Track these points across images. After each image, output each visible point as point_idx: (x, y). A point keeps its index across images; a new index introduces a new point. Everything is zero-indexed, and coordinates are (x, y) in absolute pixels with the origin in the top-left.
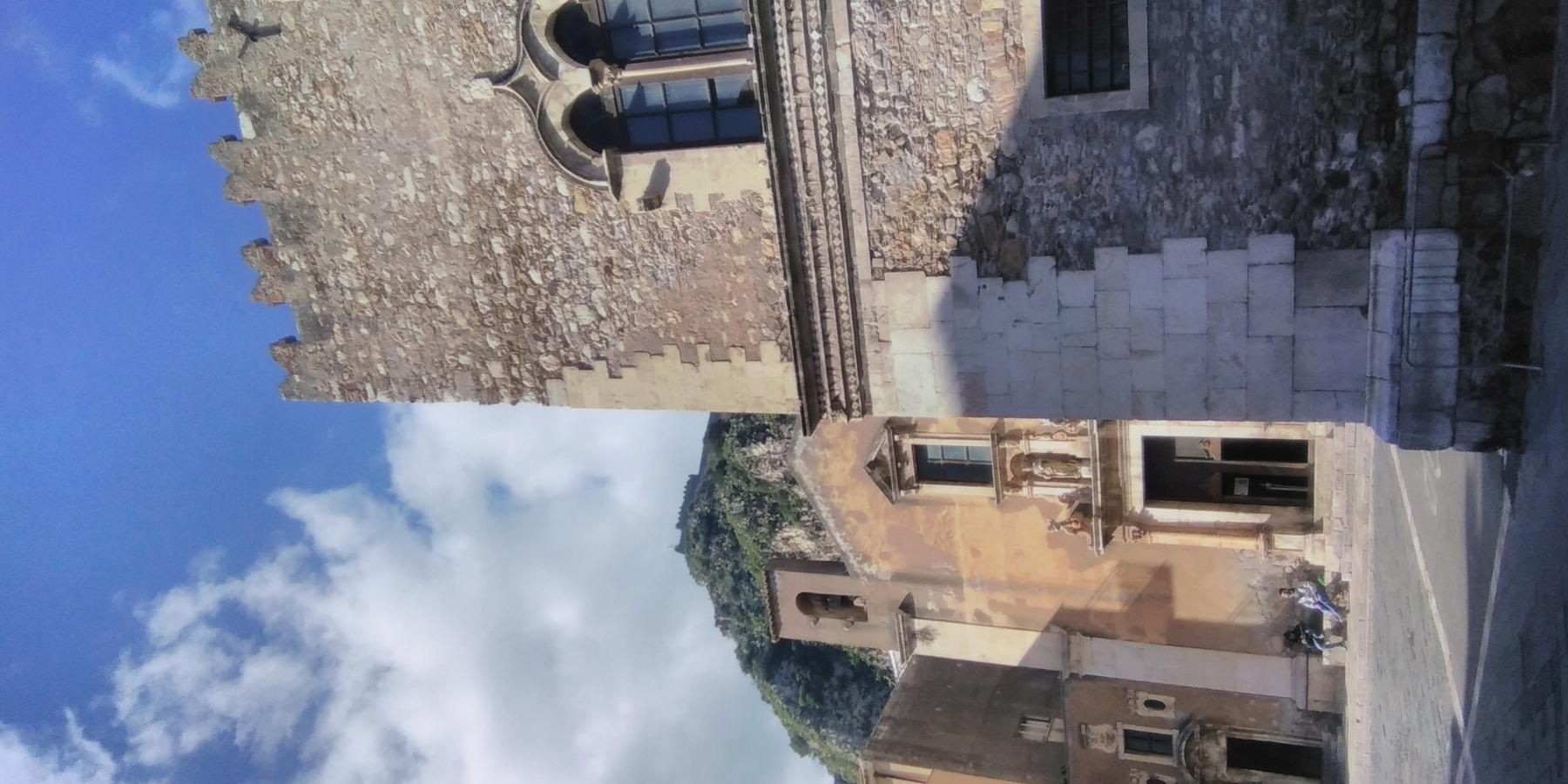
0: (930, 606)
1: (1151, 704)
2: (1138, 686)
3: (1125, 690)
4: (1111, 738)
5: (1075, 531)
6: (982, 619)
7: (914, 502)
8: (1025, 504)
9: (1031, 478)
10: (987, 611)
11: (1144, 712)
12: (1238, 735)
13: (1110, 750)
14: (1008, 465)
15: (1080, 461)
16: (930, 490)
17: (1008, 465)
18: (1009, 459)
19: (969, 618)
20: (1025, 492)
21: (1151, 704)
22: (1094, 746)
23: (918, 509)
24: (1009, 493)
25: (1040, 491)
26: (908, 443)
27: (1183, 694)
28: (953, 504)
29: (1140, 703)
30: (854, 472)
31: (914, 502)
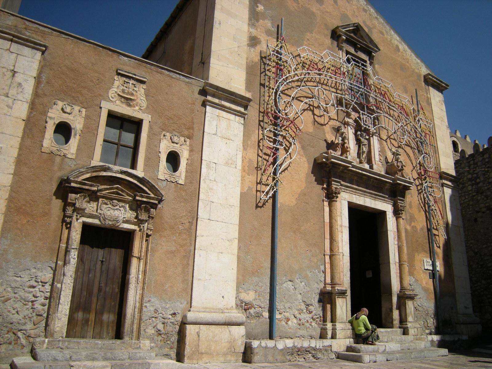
0: (260, 8)
1: (173, 159)
2: (198, 150)
3: (189, 137)
4: (128, 101)
6: (253, 41)
10: (258, 48)
11: (165, 147)
12: (138, 246)
13: (112, 93)
19: (254, 32)
21: (173, 159)
22: (118, 81)
27: (192, 192)
29: (176, 148)
30: (344, 16)
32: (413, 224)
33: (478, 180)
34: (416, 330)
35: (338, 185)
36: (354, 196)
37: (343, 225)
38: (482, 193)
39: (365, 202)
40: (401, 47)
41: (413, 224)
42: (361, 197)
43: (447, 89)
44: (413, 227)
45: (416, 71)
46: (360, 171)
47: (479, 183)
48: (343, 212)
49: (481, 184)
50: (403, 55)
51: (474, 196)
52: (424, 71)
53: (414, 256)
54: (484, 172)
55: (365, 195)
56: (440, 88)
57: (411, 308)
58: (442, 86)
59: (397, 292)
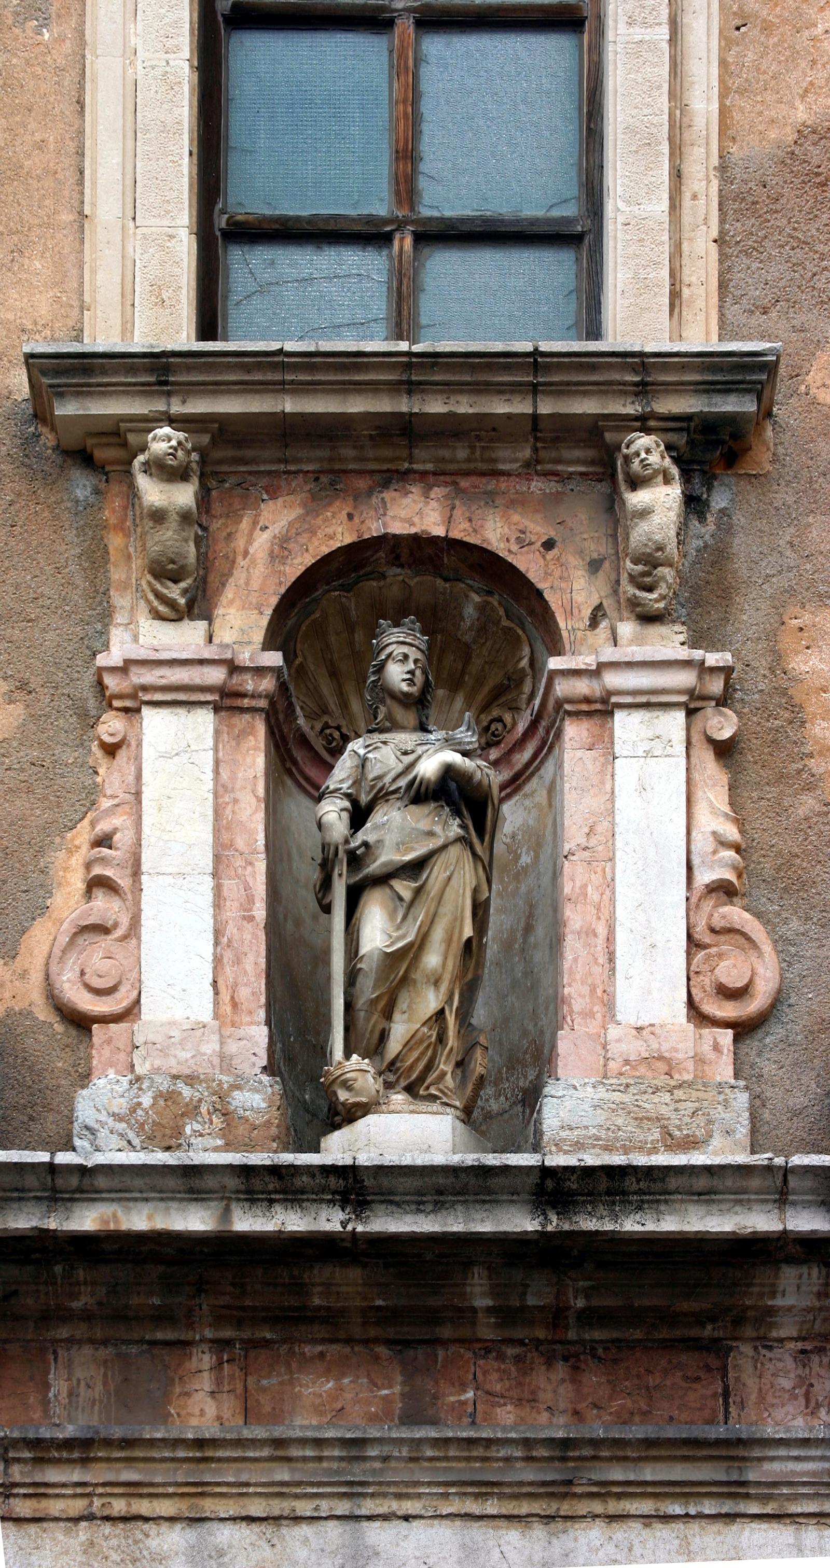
9: (299, 719)
14: (416, 513)
25: (186, 786)
42: (305, 1530)
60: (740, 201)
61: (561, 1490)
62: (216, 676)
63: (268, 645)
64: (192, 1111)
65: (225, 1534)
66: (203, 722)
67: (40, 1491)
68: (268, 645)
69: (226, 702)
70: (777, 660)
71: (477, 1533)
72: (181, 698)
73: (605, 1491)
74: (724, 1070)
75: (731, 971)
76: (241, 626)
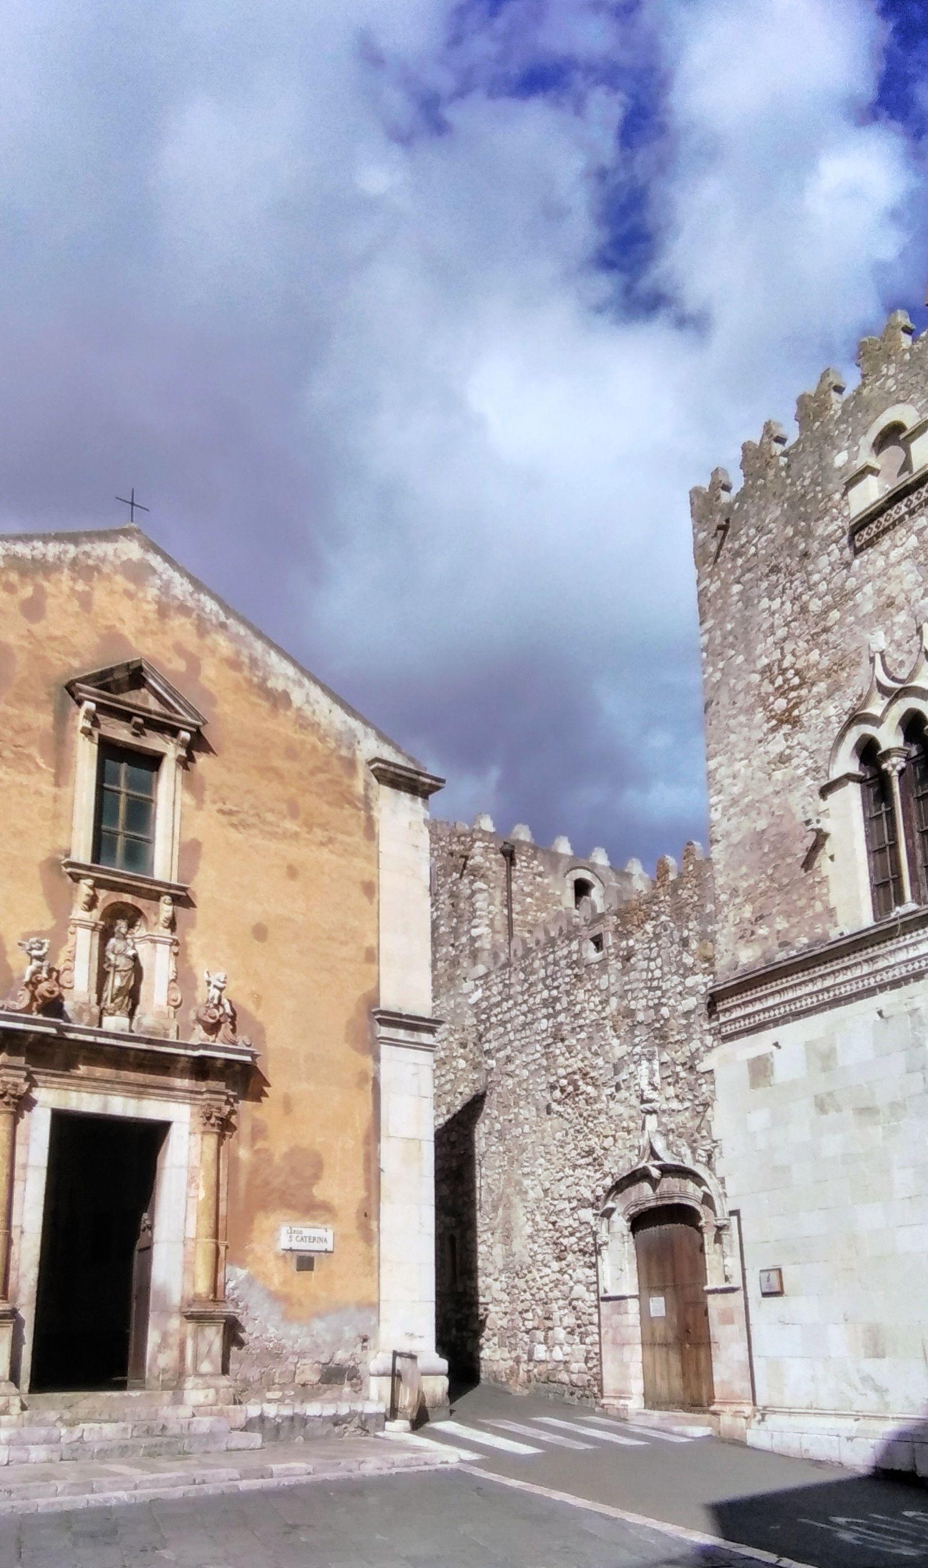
5: (33, 983)
7: (62, 719)
8: (60, 909)
9: (106, 934)
14: (127, 898)
15: (131, 1014)
16: (85, 756)
17: (127, 898)
18: (141, 903)
20: (79, 913)
23: (44, 720)
24: (85, 887)
25: (83, 943)
26: (170, 749)
28: (57, 784)
31: (62, 719)
32: (256, 1148)
33: (558, 1007)
34: (212, 1392)
35: (18, 1076)
36: (74, 1094)
37: (32, 1161)
38: (563, 1040)
39: (105, 1106)
40: (297, 697)
41: (256, 1148)
43: (438, 788)
44: (257, 1152)
45: (344, 752)
46: (90, 1038)
47: (560, 1012)
48: (34, 1135)
49: (561, 1018)
50: (301, 717)
51: (548, 1046)
52: (370, 747)
53: (252, 1221)
54: (568, 987)
55: (107, 1089)
56: (412, 784)
57: (210, 1345)
58: (424, 784)
59: (181, 1307)
60: (181, 850)
61: (141, 1093)
62: (93, 925)
63: (101, 919)
64: (84, 1011)
65: (84, 1095)
66: (89, 932)
67: (52, 1082)
68: (101, 919)
69: (93, 929)
70: (183, 937)
71: (127, 1100)
72: (86, 927)
73: (149, 1094)
74: (172, 1015)
75: (173, 996)
76: (96, 914)
